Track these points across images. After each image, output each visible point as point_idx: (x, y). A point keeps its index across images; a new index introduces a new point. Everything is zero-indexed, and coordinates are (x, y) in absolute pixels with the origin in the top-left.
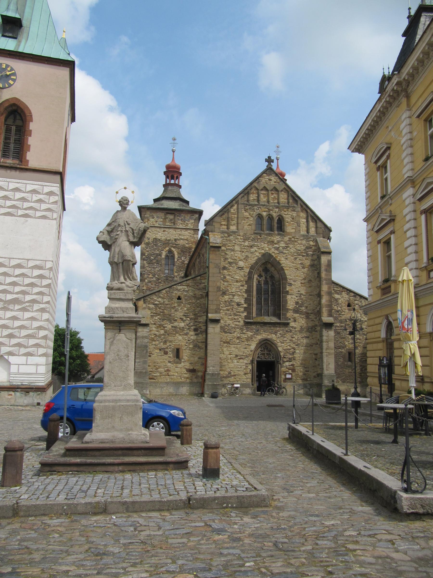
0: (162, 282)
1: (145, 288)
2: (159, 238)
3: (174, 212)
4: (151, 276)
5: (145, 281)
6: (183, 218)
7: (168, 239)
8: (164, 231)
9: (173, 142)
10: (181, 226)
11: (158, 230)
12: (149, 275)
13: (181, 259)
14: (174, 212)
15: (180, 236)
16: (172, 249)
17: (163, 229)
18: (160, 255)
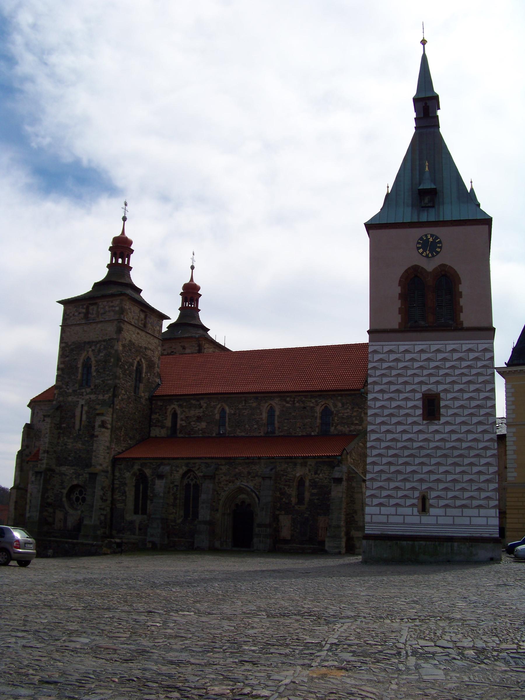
0: (132, 403)
1: (118, 407)
2: (134, 341)
3: (146, 310)
4: (123, 392)
5: (119, 398)
6: (152, 321)
7: (140, 345)
8: (138, 333)
9: (124, 206)
10: (150, 332)
11: (133, 329)
12: (122, 390)
13: (148, 375)
14: (146, 310)
15: (149, 345)
16: (143, 360)
17: (138, 331)
18: (132, 364)
